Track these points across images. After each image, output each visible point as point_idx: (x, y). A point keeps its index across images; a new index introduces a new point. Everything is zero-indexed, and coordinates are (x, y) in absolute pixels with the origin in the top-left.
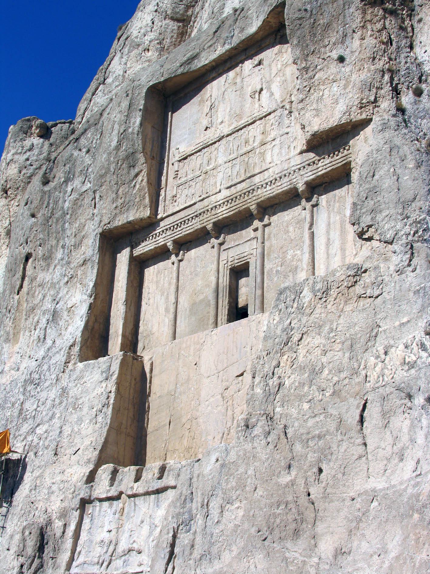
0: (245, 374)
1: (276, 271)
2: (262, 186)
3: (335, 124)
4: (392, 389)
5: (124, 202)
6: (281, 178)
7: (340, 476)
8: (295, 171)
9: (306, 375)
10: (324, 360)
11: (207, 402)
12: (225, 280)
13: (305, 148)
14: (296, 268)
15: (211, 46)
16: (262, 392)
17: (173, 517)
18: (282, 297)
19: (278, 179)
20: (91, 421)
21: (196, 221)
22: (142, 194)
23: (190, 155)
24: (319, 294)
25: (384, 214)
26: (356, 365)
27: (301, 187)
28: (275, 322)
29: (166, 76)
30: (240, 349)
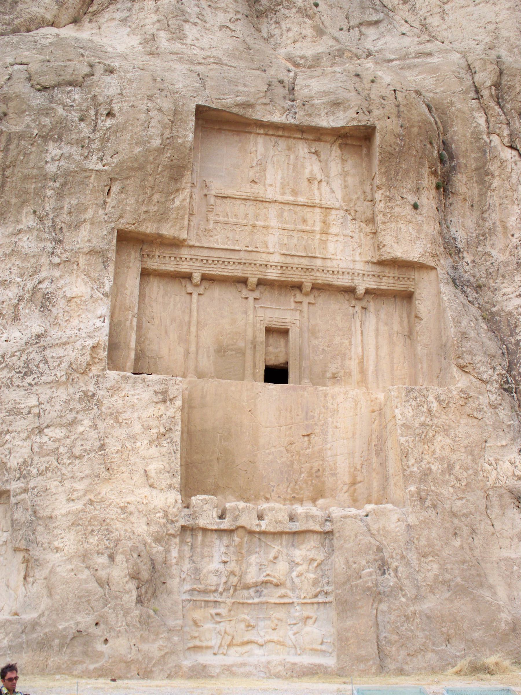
0: (313, 436)
1: (323, 349)
2: (323, 271)
3: (416, 260)
4: (506, 491)
5: (158, 210)
6: (343, 273)
7: (485, 545)
8: (359, 274)
9: (446, 465)
10: (454, 456)
11: (267, 451)
12: (262, 336)
13: (375, 261)
14: (345, 355)
15: (265, 104)
16: (419, 471)
17: (368, 562)
18: (412, 395)
19: (341, 273)
20: (151, 442)
21: (237, 268)
22: (181, 212)
23: (230, 198)
24: (444, 405)
25: (479, 358)
26: (476, 467)
27: (361, 290)
28: (410, 415)
29: (219, 107)
30: (307, 413)
